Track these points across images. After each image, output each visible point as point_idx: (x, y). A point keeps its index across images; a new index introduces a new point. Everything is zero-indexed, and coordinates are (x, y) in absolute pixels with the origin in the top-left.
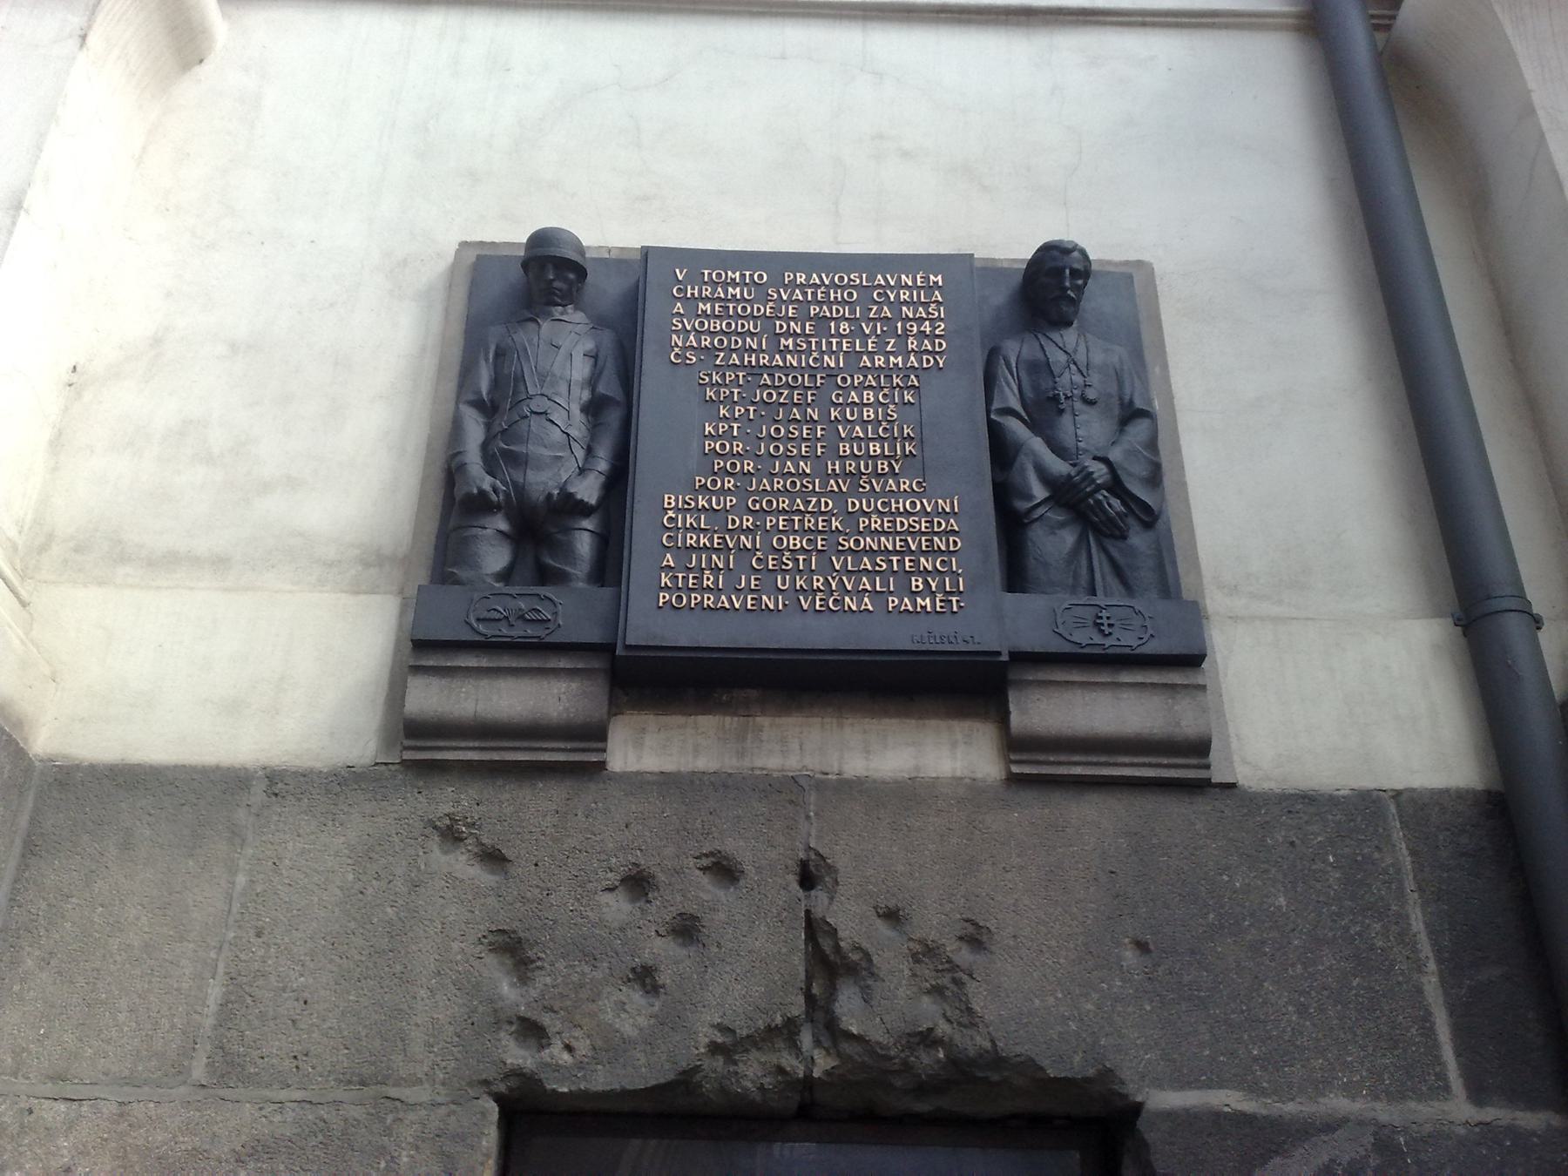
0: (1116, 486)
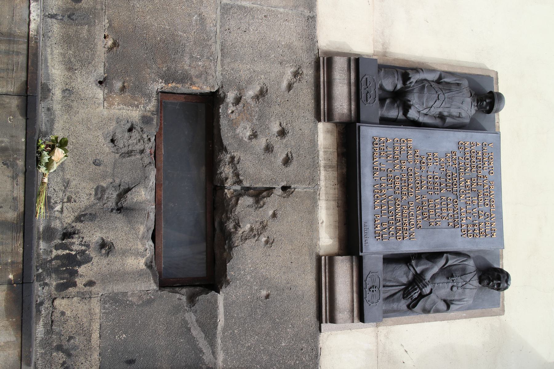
0: (421, 296)
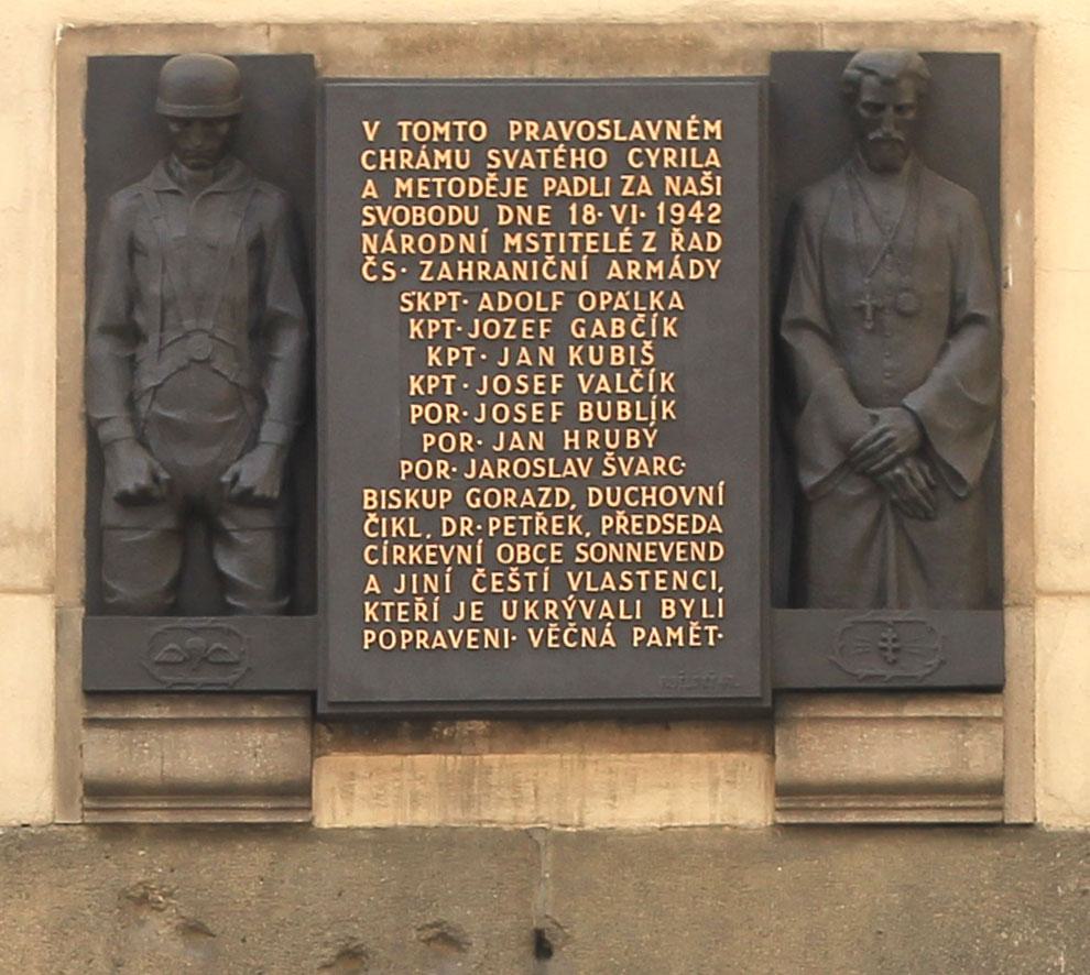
0: (924, 449)
